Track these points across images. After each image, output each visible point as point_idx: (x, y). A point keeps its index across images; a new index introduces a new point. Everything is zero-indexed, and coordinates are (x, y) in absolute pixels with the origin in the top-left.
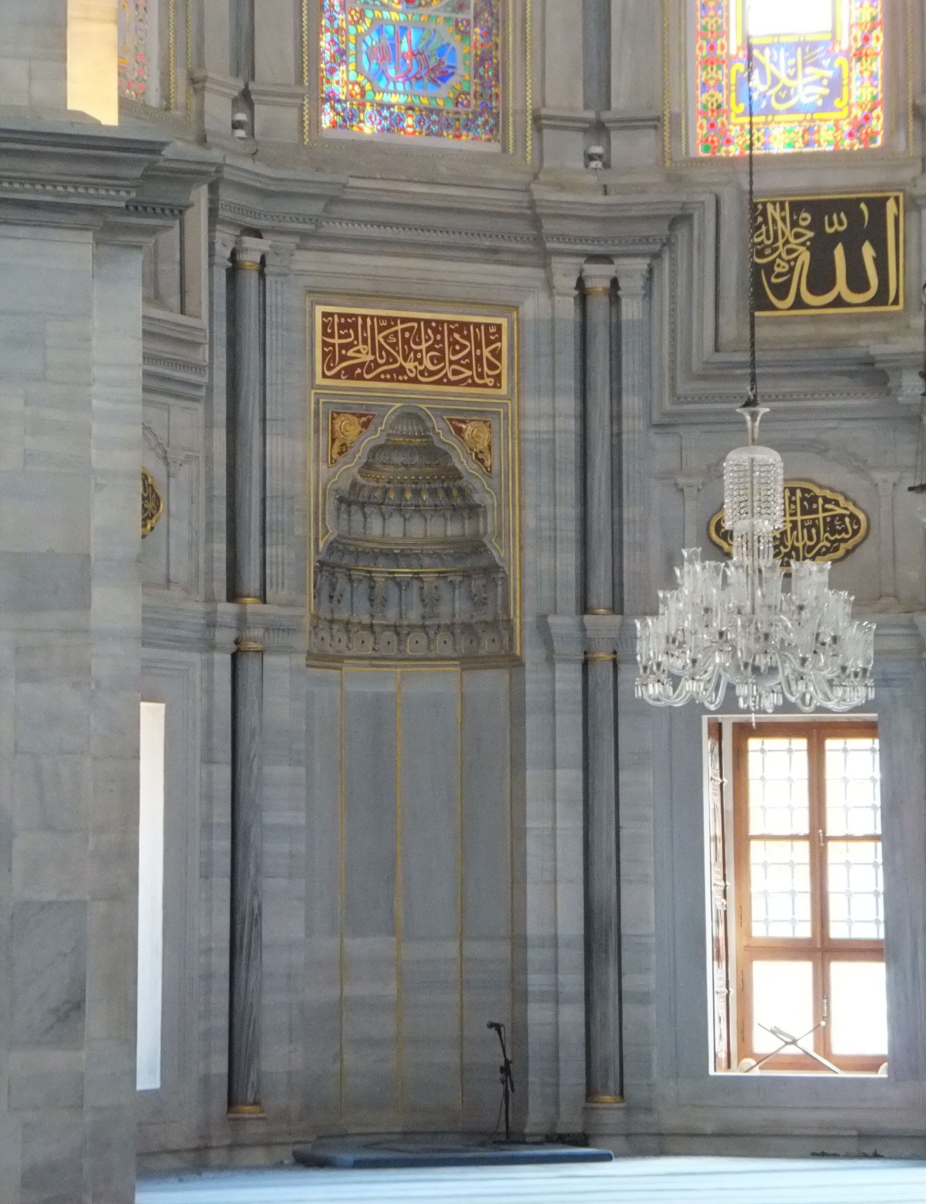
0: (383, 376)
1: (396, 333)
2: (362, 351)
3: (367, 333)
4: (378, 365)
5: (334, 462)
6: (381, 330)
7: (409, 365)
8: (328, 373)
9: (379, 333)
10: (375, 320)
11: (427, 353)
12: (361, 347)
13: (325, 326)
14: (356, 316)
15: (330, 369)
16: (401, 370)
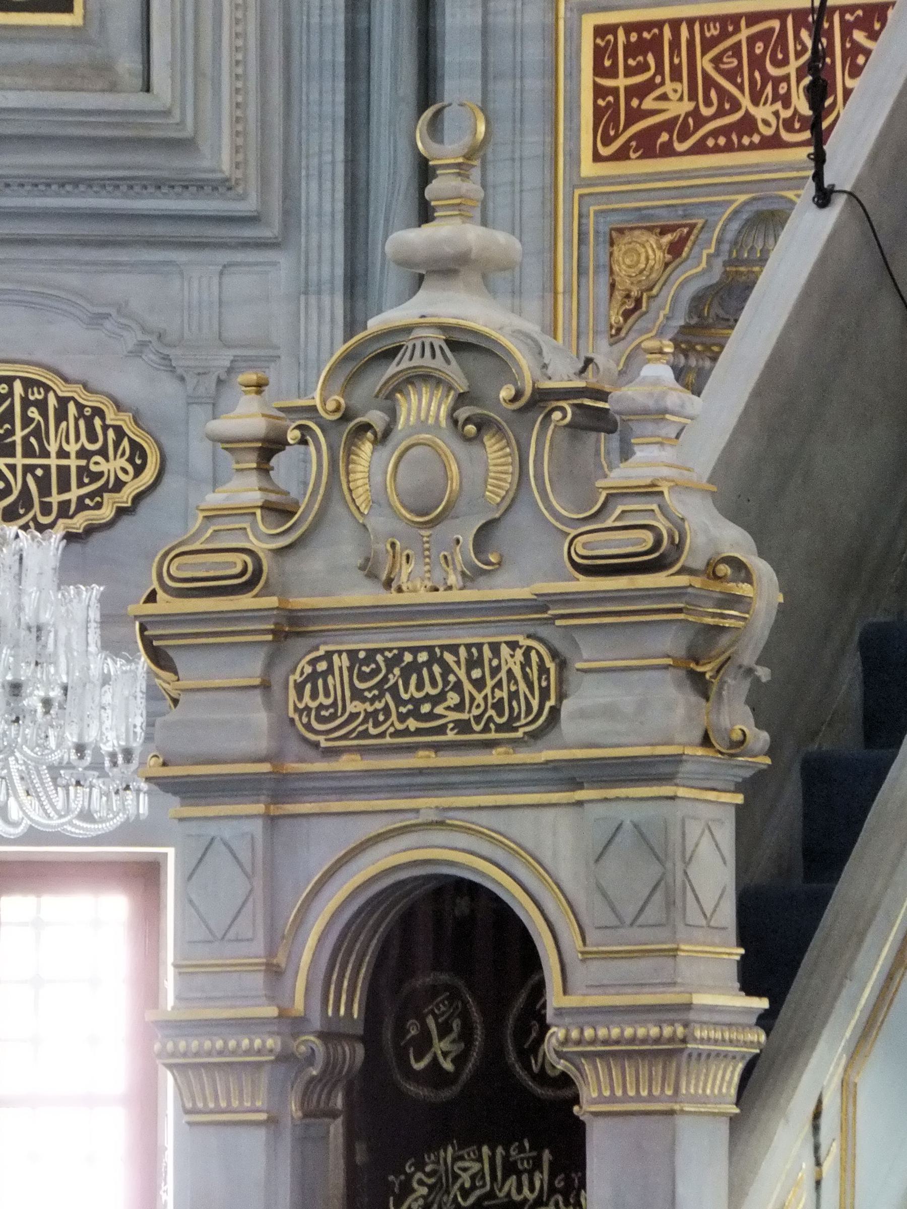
0: (710, 143)
1: (736, 49)
2: (671, 95)
3: (679, 55)
4: (701, 121)
5: (616, 335)
6: (708, 45)
7: (762, 113)
8: (604, 151)
9: (704, 53)
10: (697, 27)
11: (798, 82)
12: (669, 87)
13: (599, 53)
14: (659, 24)
15: (607, 142)
16: (748, 125)
